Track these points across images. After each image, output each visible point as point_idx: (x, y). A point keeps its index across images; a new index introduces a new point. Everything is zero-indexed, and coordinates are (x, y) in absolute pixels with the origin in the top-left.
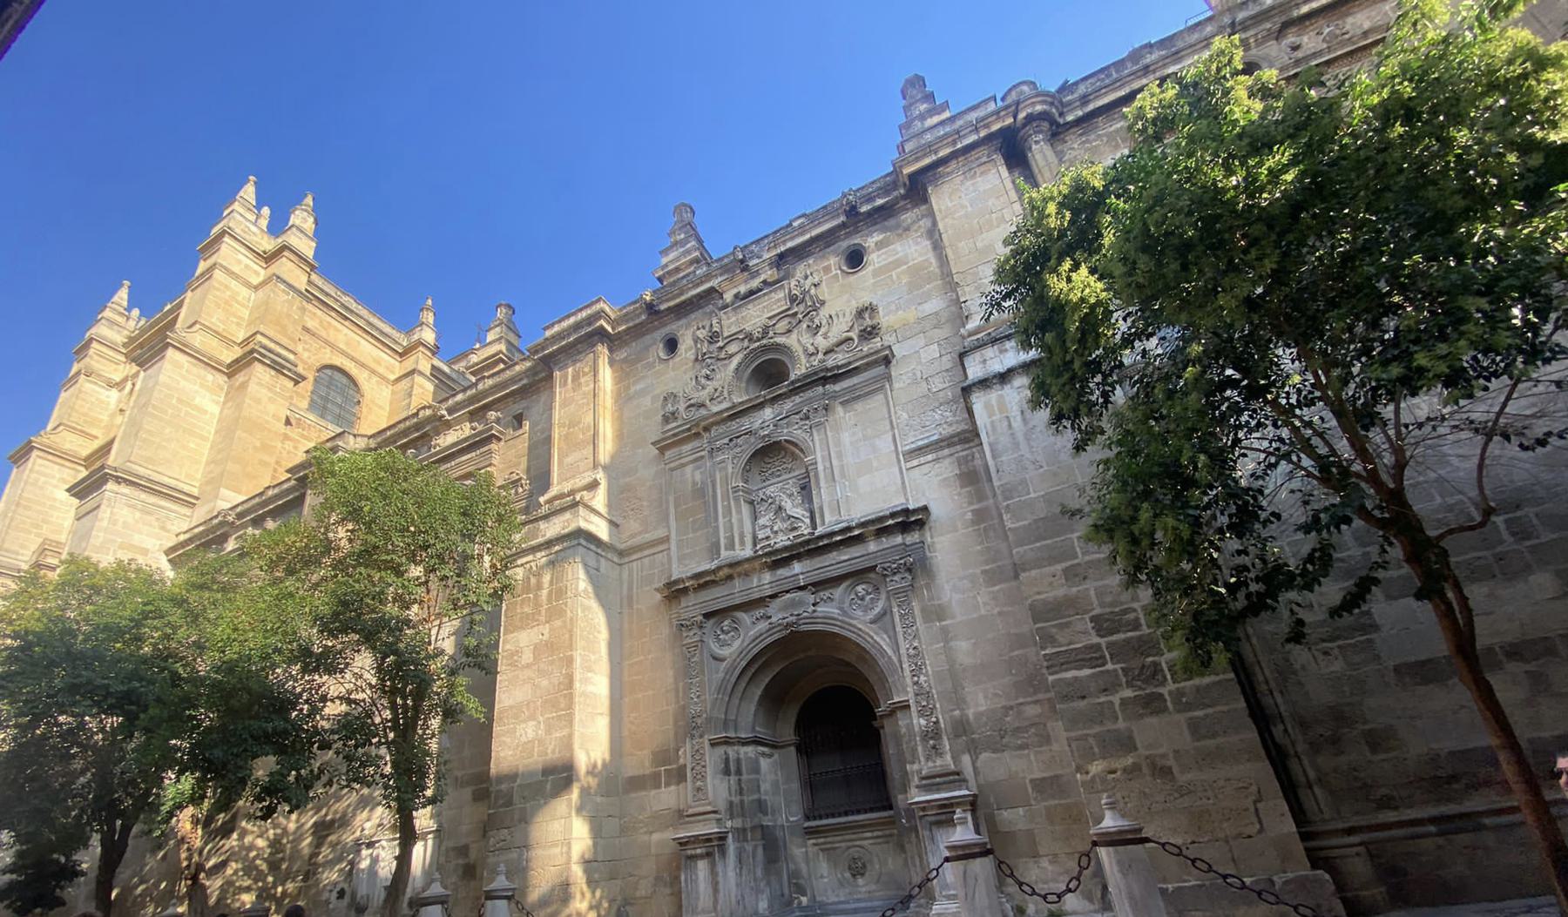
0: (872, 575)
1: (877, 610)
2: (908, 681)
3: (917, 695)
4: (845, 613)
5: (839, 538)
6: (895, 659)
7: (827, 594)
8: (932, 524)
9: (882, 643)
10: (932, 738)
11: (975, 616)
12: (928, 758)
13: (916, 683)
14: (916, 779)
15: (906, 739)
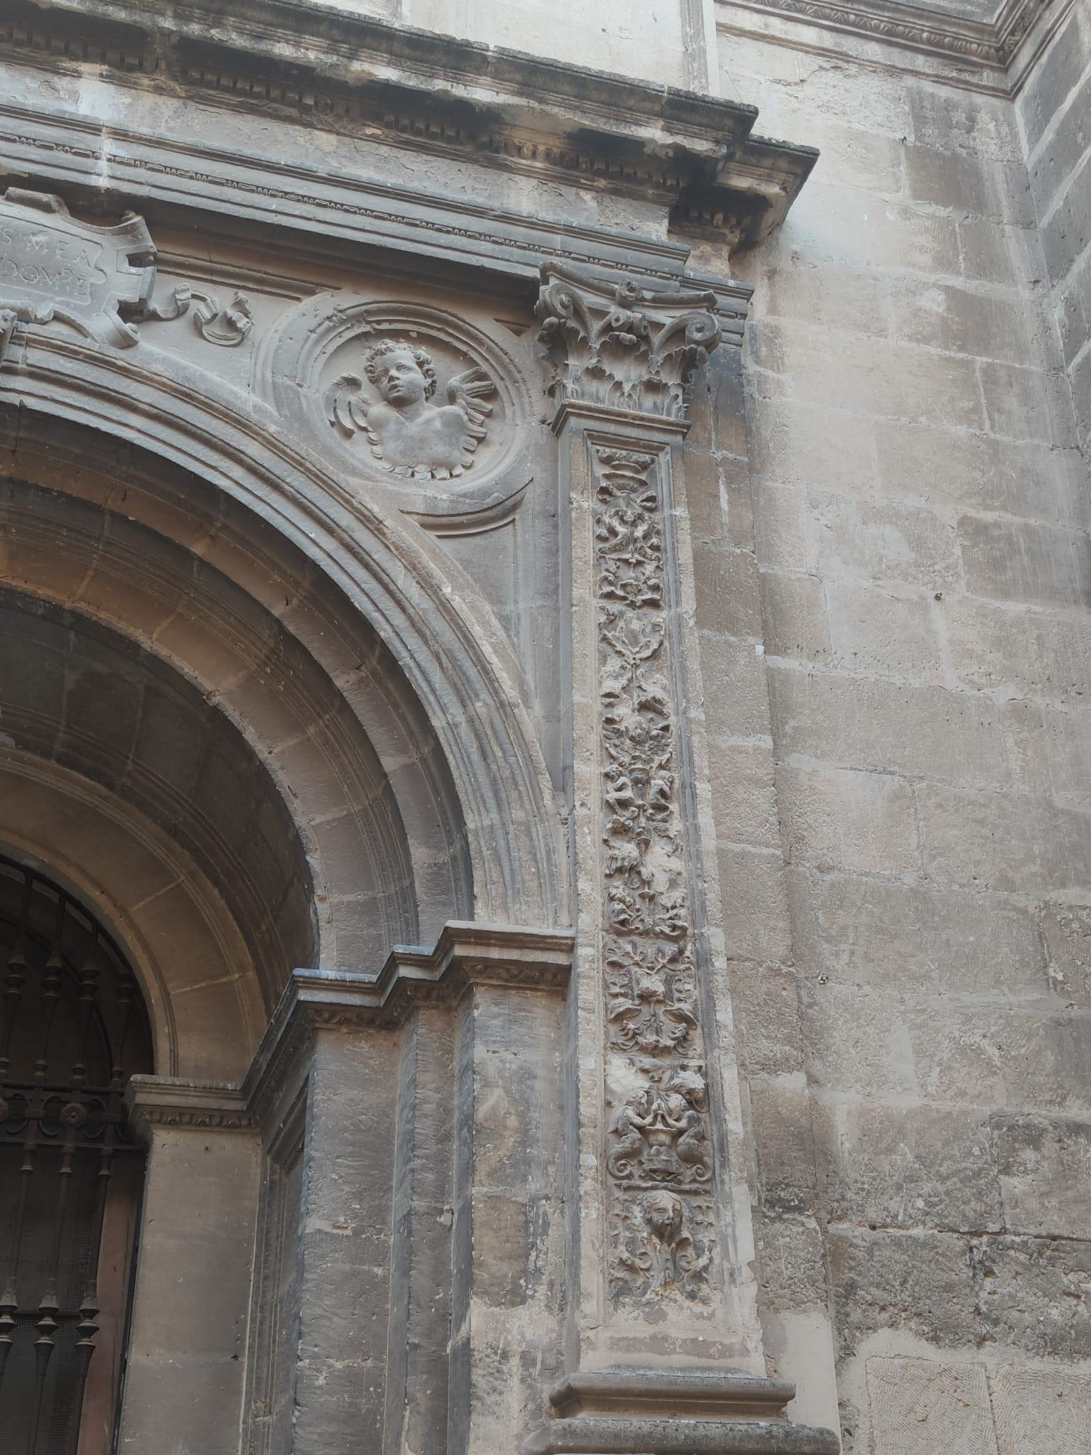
0: (488, 326)
1: (469, 482)
2: (589, 840)
3: (621, 928)
4: (300, 419)
5: (386, 73)
6: (531, 719)
7: (221, 299)
8: (785, 264)
9: (477, 630)
10: (667, 1177)
11: (916, 683)
12: (619, 1292)
13: (630, 871)
14: (514, 1397)
15: (490, 1156)
